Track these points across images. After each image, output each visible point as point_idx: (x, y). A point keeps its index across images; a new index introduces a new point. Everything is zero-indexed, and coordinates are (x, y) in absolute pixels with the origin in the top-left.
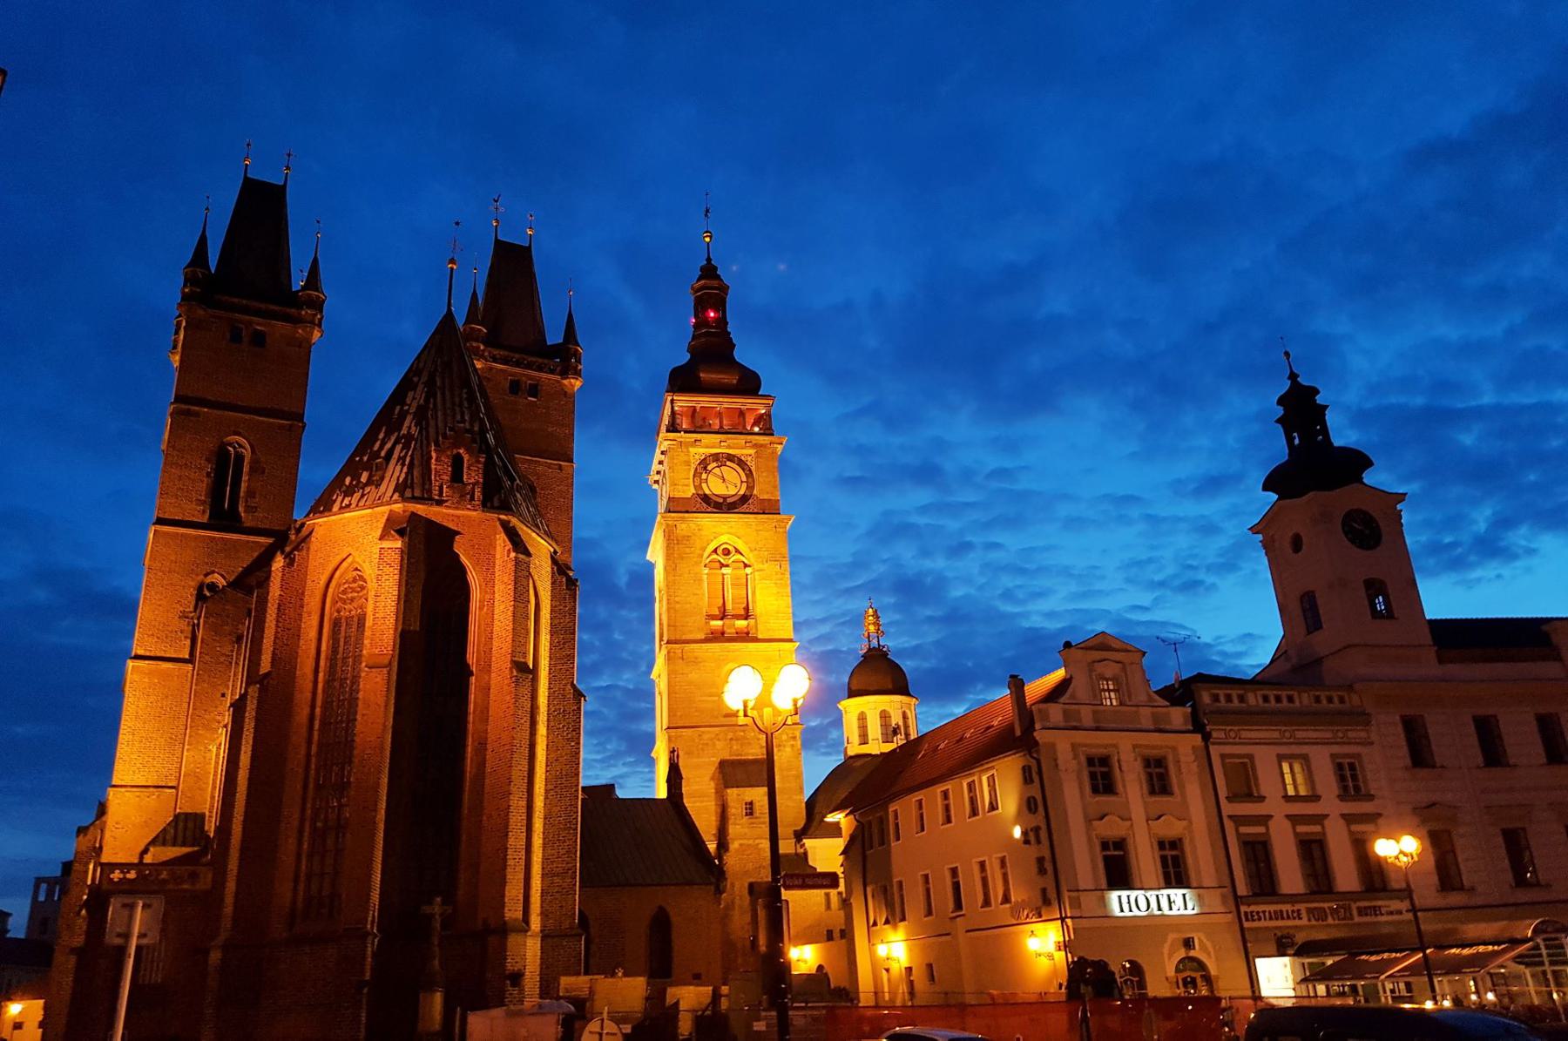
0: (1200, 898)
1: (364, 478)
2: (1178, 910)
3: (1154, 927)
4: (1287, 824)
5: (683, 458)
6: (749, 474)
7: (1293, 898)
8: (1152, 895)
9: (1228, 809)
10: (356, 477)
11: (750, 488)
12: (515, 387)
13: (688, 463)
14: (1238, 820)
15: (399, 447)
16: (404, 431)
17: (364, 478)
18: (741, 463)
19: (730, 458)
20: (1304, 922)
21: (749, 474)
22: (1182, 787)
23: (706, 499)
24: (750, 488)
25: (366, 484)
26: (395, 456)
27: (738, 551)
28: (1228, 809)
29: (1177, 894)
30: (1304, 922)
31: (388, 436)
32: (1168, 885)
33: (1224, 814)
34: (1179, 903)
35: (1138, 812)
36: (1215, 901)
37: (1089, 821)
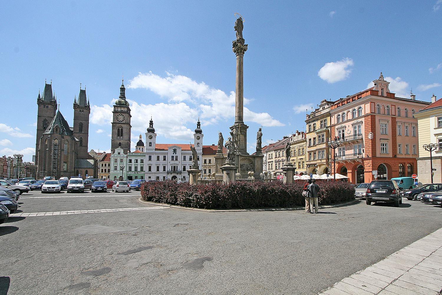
35: (119, 164)
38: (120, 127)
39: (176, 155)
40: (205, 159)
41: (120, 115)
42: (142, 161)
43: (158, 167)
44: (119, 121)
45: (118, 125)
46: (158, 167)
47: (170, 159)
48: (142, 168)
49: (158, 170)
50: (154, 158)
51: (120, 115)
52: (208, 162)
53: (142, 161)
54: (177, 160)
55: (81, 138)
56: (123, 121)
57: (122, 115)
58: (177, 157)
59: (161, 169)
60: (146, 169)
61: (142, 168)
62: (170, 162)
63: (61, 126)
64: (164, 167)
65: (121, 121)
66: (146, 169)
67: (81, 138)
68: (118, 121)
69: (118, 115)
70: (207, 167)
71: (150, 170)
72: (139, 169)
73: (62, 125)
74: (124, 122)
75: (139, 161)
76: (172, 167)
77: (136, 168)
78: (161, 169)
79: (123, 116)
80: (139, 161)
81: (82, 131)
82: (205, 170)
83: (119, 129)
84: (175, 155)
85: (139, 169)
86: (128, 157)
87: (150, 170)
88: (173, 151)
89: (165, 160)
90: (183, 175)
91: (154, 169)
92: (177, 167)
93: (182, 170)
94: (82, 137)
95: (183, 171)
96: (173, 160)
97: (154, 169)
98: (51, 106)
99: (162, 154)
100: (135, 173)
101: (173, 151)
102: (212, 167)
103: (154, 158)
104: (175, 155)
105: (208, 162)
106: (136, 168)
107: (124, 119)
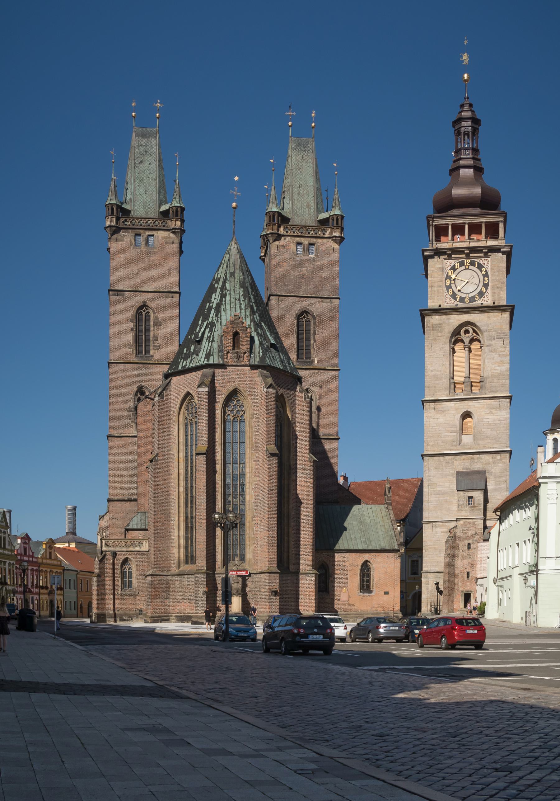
1: (192, 350)
10: (189, 349)
15: (207, 330)
16: (210, 320)
17: (192, 350)
25: (193, 353)
26: (206, 336)
31: (203, 321)
38: (467, 332)
41: (462, 264)
44: (462, 300)
45: (456, 320)
51: (462, 264)
56: (481, 294)
57: (472, 264)
63: (253, 321)
65: (472, 299)
68: (454, 296)
69: (453, 269)
73: (257, 317)
74: (487, 301)
79: (480, 267)
81: (308, 355)
98: (166, 234)
107: (486, 286)
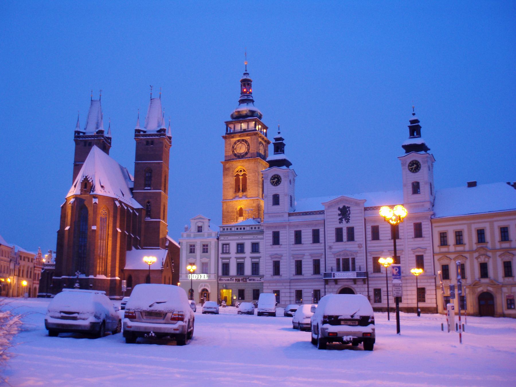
0: (209, 277)
2: (202, 278)
3: (199, 282)
4: (250, 259)
5: (229, 143)
6: (248, 145)
7: (233, 276)
8: (199, 275)
9: (221, 256)
11: (248, 150)
12: (148, 143)
13: (230, 144)
14: (223, 258)
18: (246, 142)
19: (243, 140)
20: (234, 282)
21: (248, 145)
22: (210, 251)
23: (235, 155)
24: (248, 150)
27: (244, 171)
28: (221, 256)
29: (203, 275)
30: (234, 282)
32: (203, 273)
33: (219, 257)
34: (204, 277)
36: (213, 277)
37: (201, 258)
39: (350, 225)
40: (442, 229)
42: (255, 248)
43: (299, 266)
46: (299, 266)
47: (331, 236)
48: (255, 267)
49: (299, 270)
50: (287, 237)
52: (451, 239)
53: (255, 248)
54: (351, 237)
55: (149, 202)
58: (351, 232)
59: (308, 268)
60: (266, 268)
61: (255, 267)
62: (330, 248)
64: (317, 264)
66: (266, 268)
67: (149, 202)
70: (452, 256)
71: (277, 270)
72: (248, 270)
75: (248, 248)
76: (338, 260)
77: (240, 267)
78: (308, 268)
80: (248, 248)
82: (445, 270)
83: (238, 176)
84: (344, 226)
85: (248, 270)
86: (222, 238)
87: (277, 270)
88: (339, 215)
89: (316, 238)
90: (374, 284)
91: (287, 269)
92: (353, 260)
93: (371, 269)
94: (150, 200)
95: (374, 272)
96: (339, 237)
97: (287, 269)
99: (308, 225)
100: (239, 280)
101: (339, 215)
102: (467, 255)
103: (287, 237)
104: (344, 226)
105: (451, 239)
106: (240, 267)
